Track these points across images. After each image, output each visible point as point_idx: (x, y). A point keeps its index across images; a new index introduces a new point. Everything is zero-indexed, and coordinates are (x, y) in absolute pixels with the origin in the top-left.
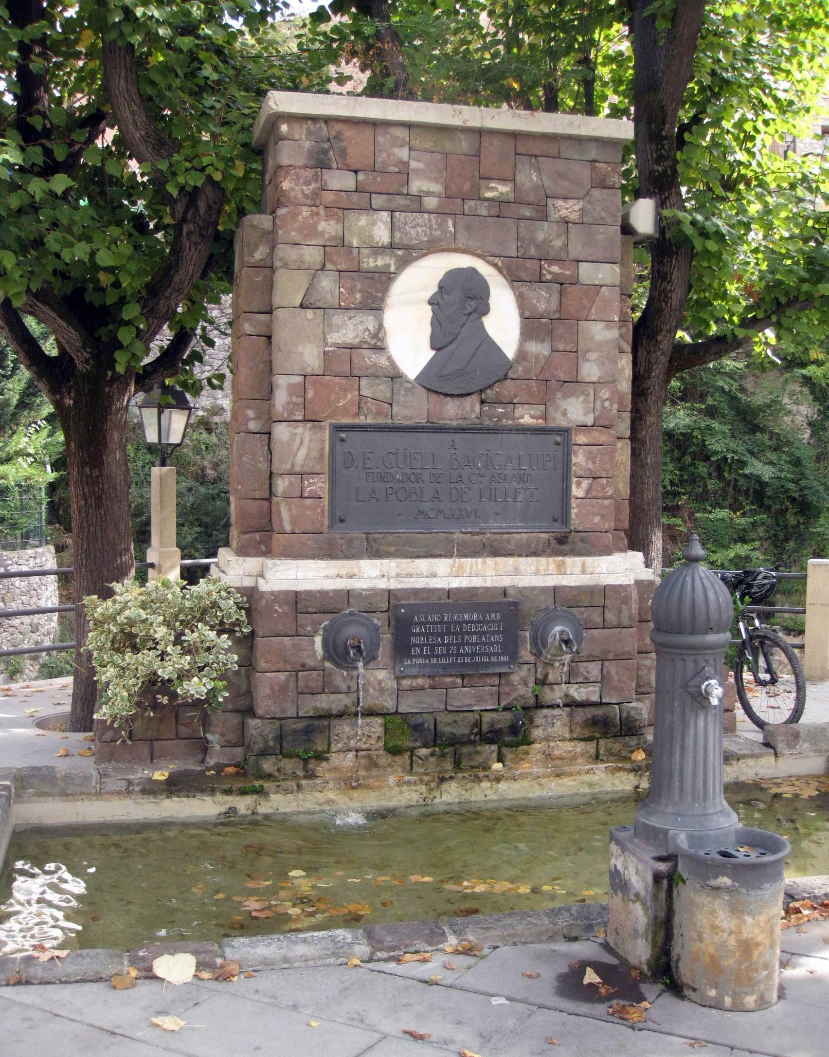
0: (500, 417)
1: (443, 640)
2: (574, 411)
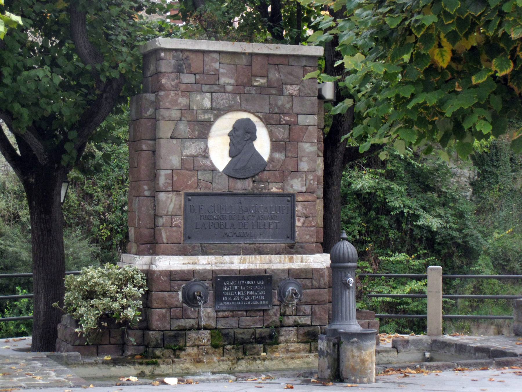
0: (262, 188)
1: (237, 293)
2: (296, 185)
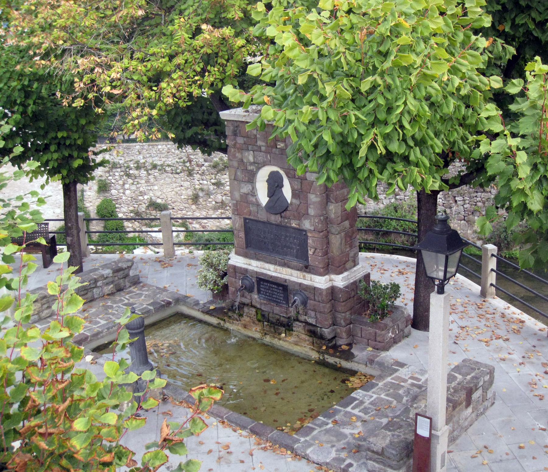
0: (287, 223)
2: (307, 225)
